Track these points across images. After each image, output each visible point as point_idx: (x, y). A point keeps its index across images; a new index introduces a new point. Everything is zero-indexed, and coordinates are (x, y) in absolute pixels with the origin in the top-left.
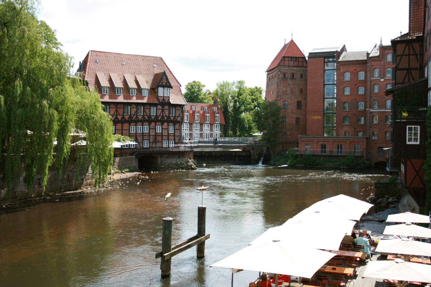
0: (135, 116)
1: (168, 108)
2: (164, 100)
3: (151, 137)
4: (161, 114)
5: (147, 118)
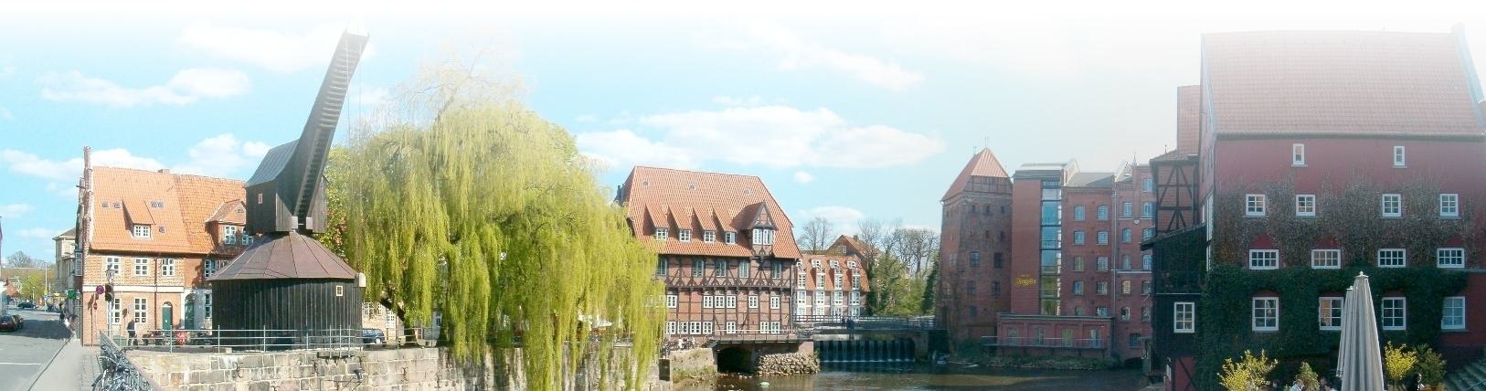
0: (712, 279)
1: (769, 265)
2: (762, 250)
3: (739, 315)
4: (758, 277)
5: (733, 283)
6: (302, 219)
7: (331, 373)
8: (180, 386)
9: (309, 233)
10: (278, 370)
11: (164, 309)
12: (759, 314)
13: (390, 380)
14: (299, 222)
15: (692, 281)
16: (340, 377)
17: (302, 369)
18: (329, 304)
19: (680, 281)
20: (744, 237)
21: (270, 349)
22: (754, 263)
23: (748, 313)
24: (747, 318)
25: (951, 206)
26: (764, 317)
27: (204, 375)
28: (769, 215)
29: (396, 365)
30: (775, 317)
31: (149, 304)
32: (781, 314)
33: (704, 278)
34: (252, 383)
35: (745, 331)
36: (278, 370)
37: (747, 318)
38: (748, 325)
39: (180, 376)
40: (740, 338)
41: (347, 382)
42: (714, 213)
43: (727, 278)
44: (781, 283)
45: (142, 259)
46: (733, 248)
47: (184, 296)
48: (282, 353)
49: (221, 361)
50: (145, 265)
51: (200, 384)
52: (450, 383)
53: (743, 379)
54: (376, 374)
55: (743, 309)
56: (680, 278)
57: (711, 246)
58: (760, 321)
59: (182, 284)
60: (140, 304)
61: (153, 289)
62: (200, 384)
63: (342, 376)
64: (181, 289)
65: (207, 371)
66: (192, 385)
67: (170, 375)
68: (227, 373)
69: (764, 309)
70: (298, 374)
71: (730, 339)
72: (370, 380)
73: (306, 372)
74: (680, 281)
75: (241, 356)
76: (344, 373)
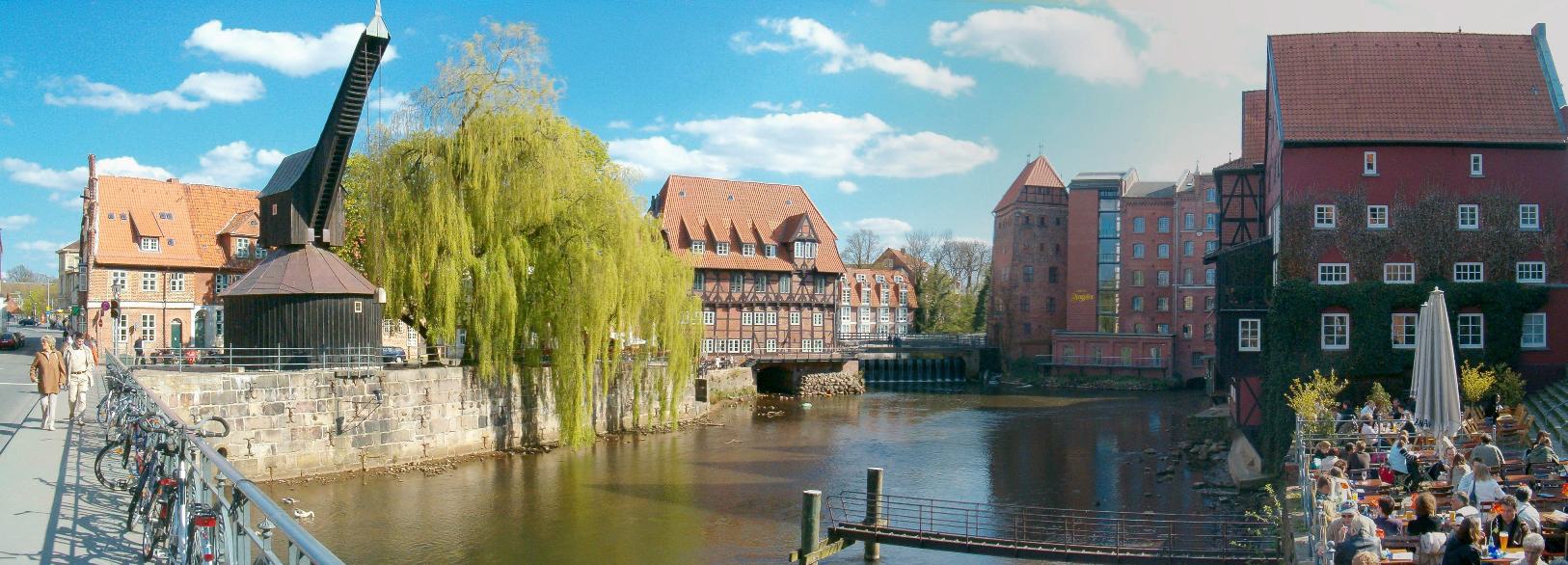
0: (752, 295)
1: (811, 280)
2: (804, 264)
3: (780, 333)
4: (800, 292)
5: (773, 299)
6: (319, 232)
7: (349, 394)
8: (190, 408)
9: (326, 246)
10: (293, 390)
11: (173, 326)
12: (801, 331)
13: (412, 401)
14: (316, 234)
15: (730, 297)
16: (358, 398)
17: (319, 389)
18: (347, 321)
19: (717, 297)
20: (785, 249)
21: (285, 368)
22: (795, 277)
23: (789, 331)
24: (789, 336)
25: (1003, 218)
26: (806, 335)
27: (215, 396)
28: (811, 227)
29: (418, 386)
30: (818, 335)
31: (158, 321)
32: (824, 331)
33: (743, 293)
34: (266, 404)
35: (786, 349)
36: (293, 390)
37: (789, 336)
38: (789, 343)
39: (190, 397)
40: (781, 357)
41: (366, 404)
42: (753, 225)
43: (767, 293)
44: (824, 299)
45: (149, 273)
46: (774, 262)
47: (194, 313)
48: (298, 373)
49: (234, 381)
50: (153, 279)
51: (211, 406)
52: (475, 405)
53: (784, 400)
54: (396, 394)
55: (784, 326)
56: (718, 293)
57: (751, 259)
58: (802, 339)
59: (192, 300)
60: (148, 321)
61: (161, 305)
62: (211, 406)
63: (361, 396)
64: (190, 305)
65: (218, 391)
66: (203, 406)
67: (179, 396)
68: (240, 393)
69: (806, 326)
70: (314, 395)
71: (770, 358)
72: (391, 402)
73: (323, 393)
74: (717, 297)
75: (255, 376)
76: (363, 393)
